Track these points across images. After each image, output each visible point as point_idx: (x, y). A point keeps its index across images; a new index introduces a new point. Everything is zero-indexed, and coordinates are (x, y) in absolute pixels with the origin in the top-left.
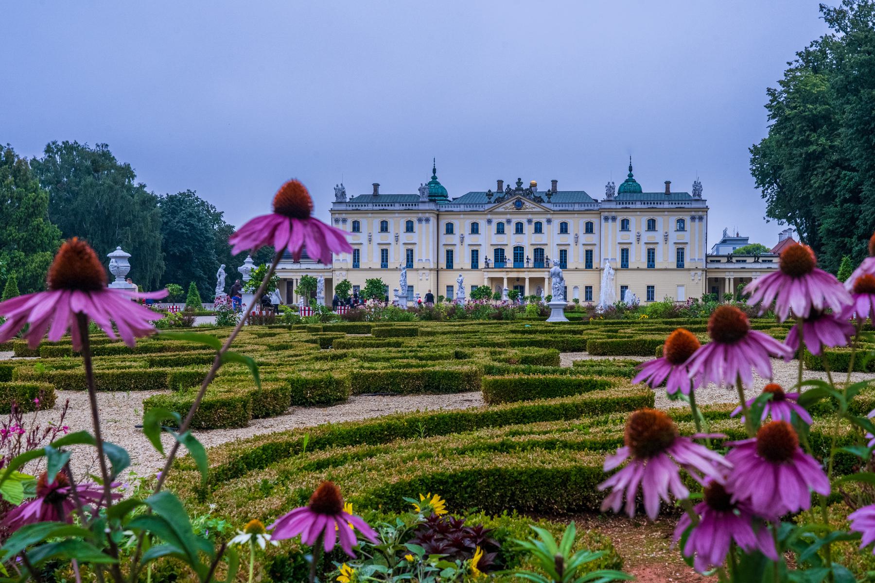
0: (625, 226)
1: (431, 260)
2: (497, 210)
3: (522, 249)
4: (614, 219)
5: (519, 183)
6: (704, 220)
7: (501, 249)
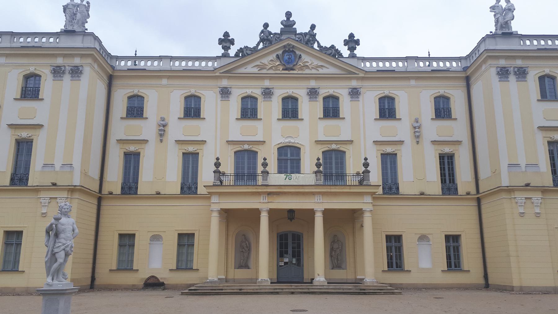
2: (242, 70)
4: (521, 73)
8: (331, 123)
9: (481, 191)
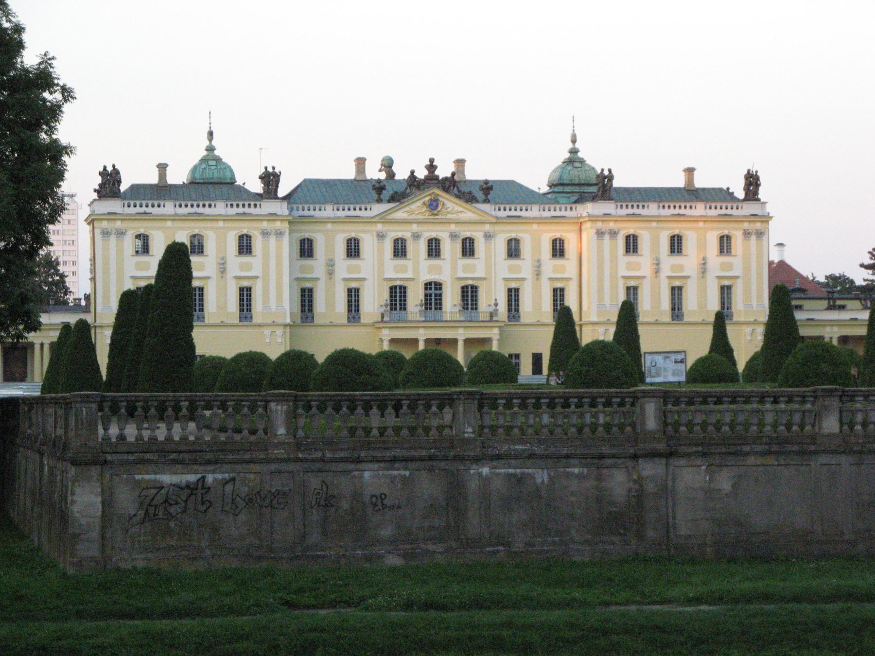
0: (632, 245)
1: (286, 305)
3: (438, 286)
4: (613, 234)
5: (431, 167)
6: (765, 238)
7: (401, 287)
8: (468, 261)
9: (583, 319)
